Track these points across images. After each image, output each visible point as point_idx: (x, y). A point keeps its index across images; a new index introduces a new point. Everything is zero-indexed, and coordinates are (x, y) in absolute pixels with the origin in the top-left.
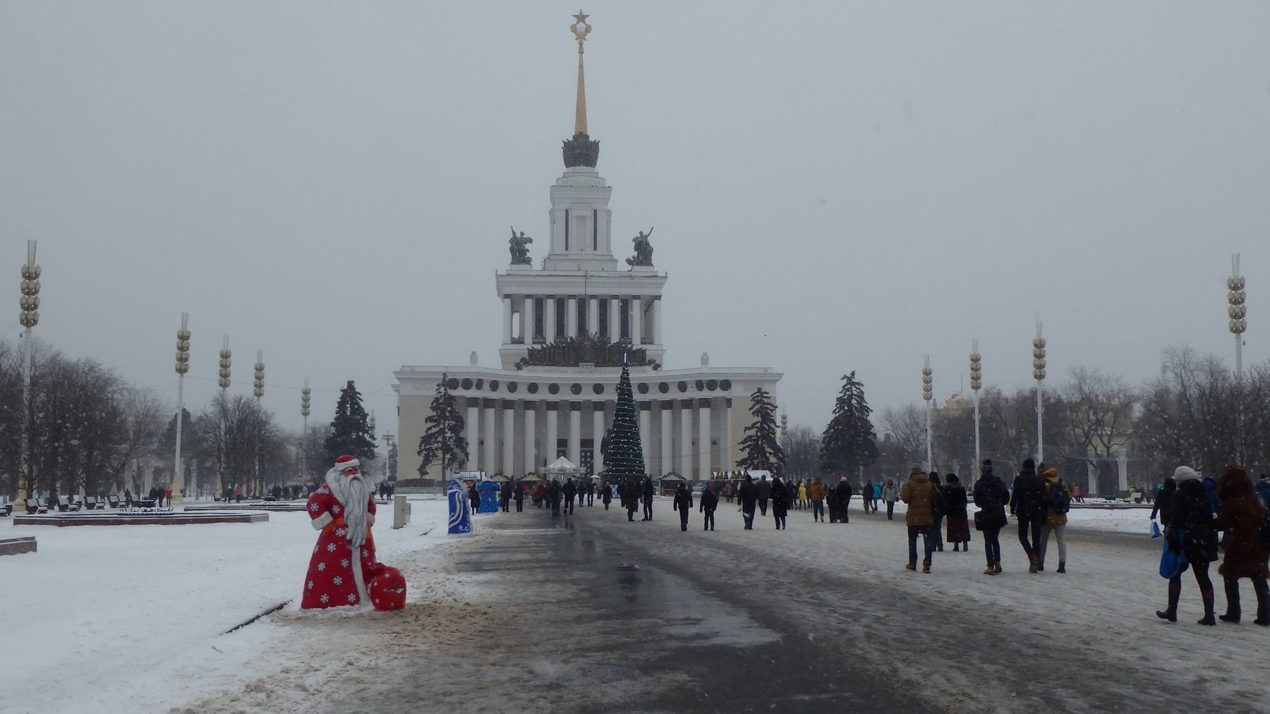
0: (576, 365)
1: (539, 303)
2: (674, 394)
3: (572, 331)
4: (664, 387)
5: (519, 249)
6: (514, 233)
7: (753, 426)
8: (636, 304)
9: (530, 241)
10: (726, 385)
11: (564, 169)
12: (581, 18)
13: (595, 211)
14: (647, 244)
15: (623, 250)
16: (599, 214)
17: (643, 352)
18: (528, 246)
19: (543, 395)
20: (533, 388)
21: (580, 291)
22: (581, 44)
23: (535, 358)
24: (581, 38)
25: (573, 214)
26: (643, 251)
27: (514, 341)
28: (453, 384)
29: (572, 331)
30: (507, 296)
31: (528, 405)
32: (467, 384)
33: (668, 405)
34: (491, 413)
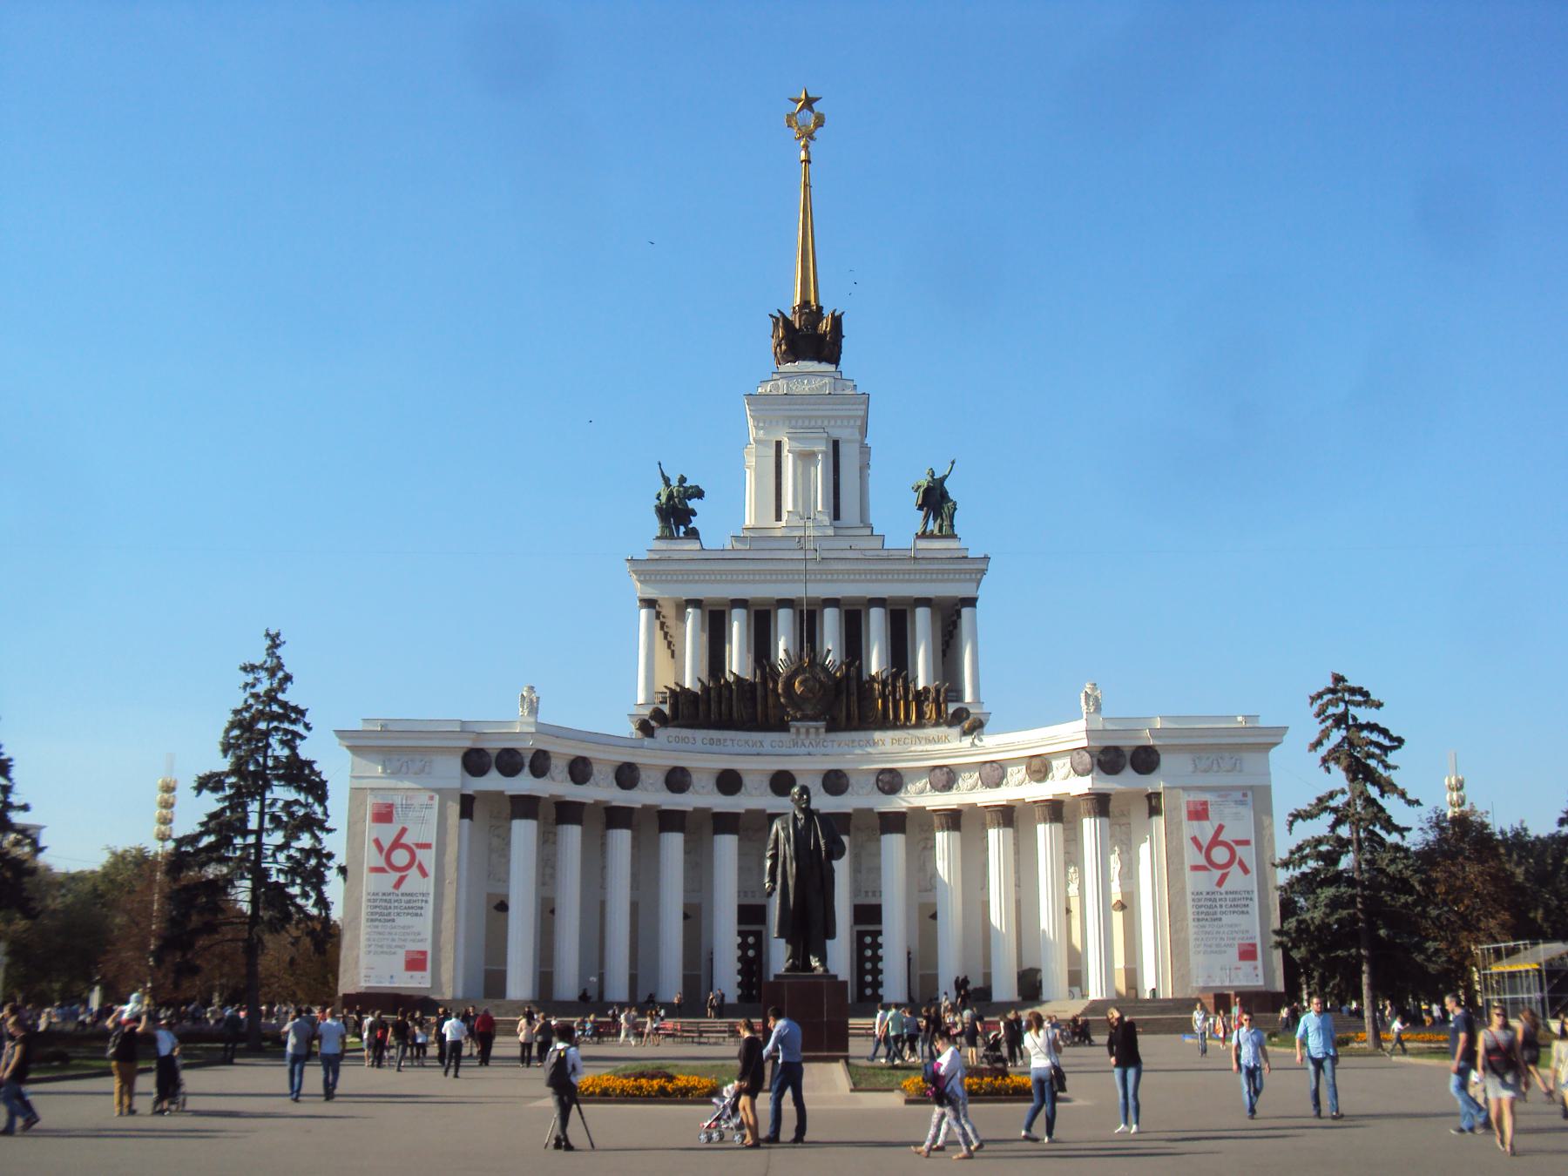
0: (783, 727)
2: (1018, 789)
4: (994, 773)
6: (667, 481)
7: (1321, 805)
8: (922, 616)
9: (699, 494)
10: (1145, 760)
13: (836, 444)
14: (944, 496)
16: (843, 449)
18: (693, 504)
19: (703, 797)
20: (677, 780)
22: (806, 147)
28: (475, 762)
31: (670, 820)
32: (509, 762)
33: (1007, 815)
34: (572, 835)
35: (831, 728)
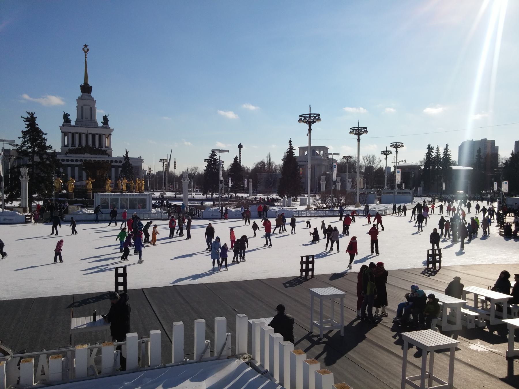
1: (73, 135)
3: (84, 144)
5: (66, 117)
8: (104, 137)
11: (81, 94)
12: (86, 46)
15: (99, 120)
17: (106, 151)
21: (86, 132)
23: (71, 152)
24: (86, 52)
25: (84, 107)
26: (106, 120)
27: (65, 146)
29: (84, 144)
30: (62, 132)
35: (91, 154)
